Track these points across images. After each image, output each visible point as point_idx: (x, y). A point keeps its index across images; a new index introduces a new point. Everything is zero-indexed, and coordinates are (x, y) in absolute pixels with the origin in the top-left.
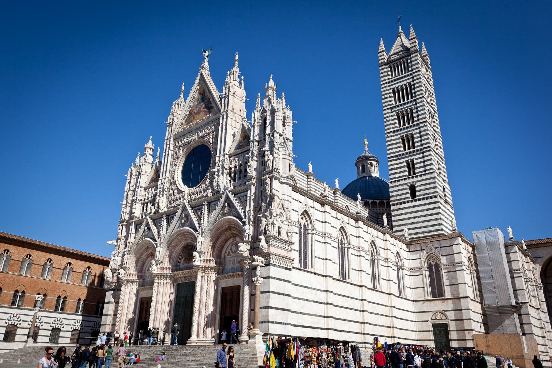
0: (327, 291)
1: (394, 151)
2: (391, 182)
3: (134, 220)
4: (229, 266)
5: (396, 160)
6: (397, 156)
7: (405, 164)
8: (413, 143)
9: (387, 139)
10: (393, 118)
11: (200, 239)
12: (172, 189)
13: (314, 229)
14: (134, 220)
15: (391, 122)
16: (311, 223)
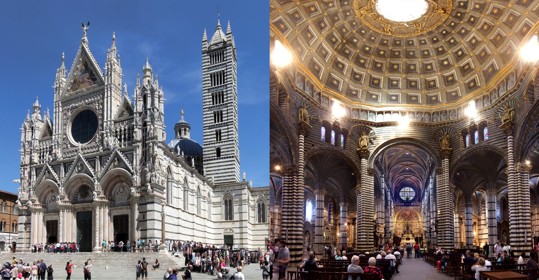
0: (178, 218)
1: (208, 122)
2: (205, 145)
3: (35, 165)
4: (118, 202)
5: (209, 129)
6: (209, 126)
7: (215, 133)
8: (222, 118)
9: (204, 113)
10: (210, 97)
11: (96, 183)
12: (65, 144)
13: (173, 179)
14: (35, 165)
15: (208, 100)
16: (171, 175)
